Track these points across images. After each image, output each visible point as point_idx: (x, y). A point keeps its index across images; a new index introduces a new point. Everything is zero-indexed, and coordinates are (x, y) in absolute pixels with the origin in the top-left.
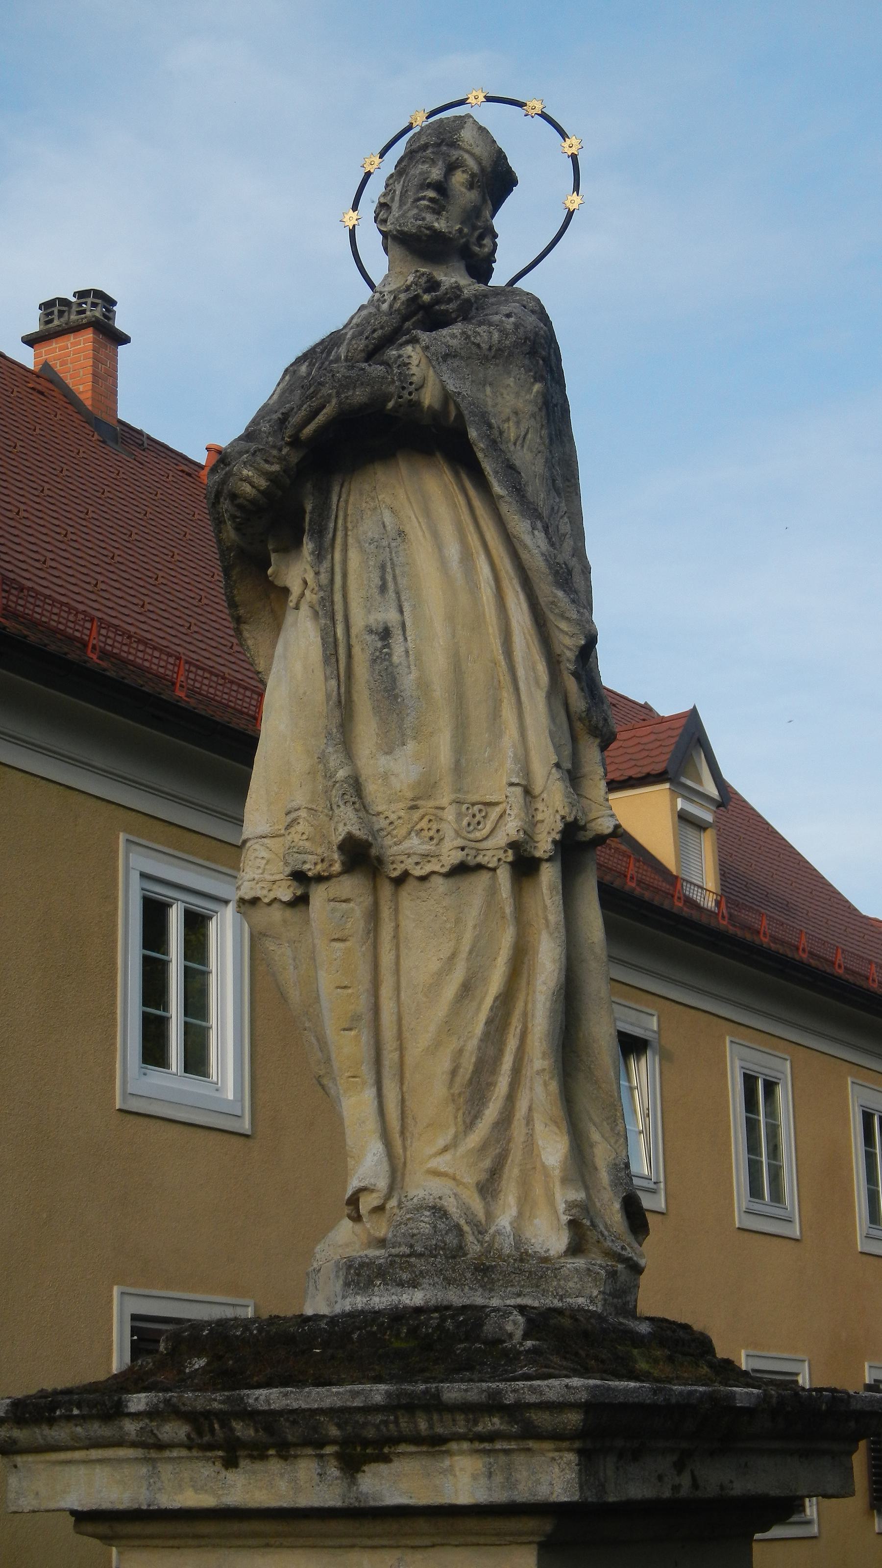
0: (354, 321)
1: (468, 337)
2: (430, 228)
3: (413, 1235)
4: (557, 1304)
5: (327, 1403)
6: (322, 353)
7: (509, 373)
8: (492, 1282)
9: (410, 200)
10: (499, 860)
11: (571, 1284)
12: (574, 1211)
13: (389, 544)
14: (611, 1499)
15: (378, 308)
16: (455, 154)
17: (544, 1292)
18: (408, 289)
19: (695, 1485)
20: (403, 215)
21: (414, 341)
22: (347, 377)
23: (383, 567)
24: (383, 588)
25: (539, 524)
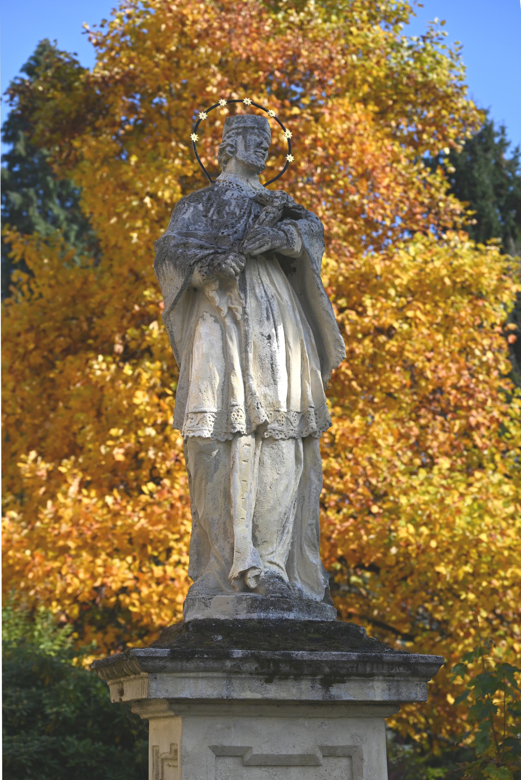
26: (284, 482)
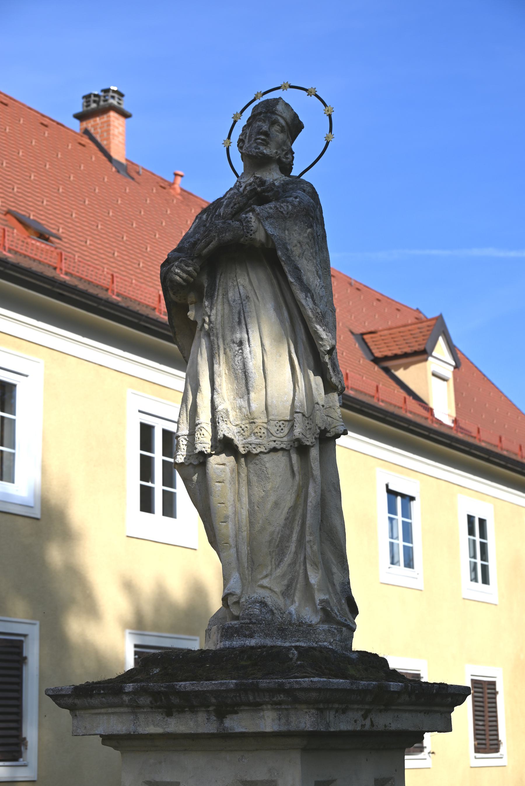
0: (228, 195)
1: (277, 208)
2: (262, 153)
3: (251, 615)
4: (315, 645)
5: (210, 688)
6: (213, 209)
7: (296, 225)
8: (286, 635)
9: (253, 139)
10: (291, 446)
11: (321, 636)
12: (323, 604)
13: (242, 303)
14: (332, 730)
15: (238, 190)
16: (274, 117)
17: (309, 640)
18: (250, 184)
19: (372, 725)
20: (249, 146)
21: (253, 211)
22: (222, 228)
23: (239, 313)
24: (239, 323)
25: (309, 295)
26: (272, 498)
